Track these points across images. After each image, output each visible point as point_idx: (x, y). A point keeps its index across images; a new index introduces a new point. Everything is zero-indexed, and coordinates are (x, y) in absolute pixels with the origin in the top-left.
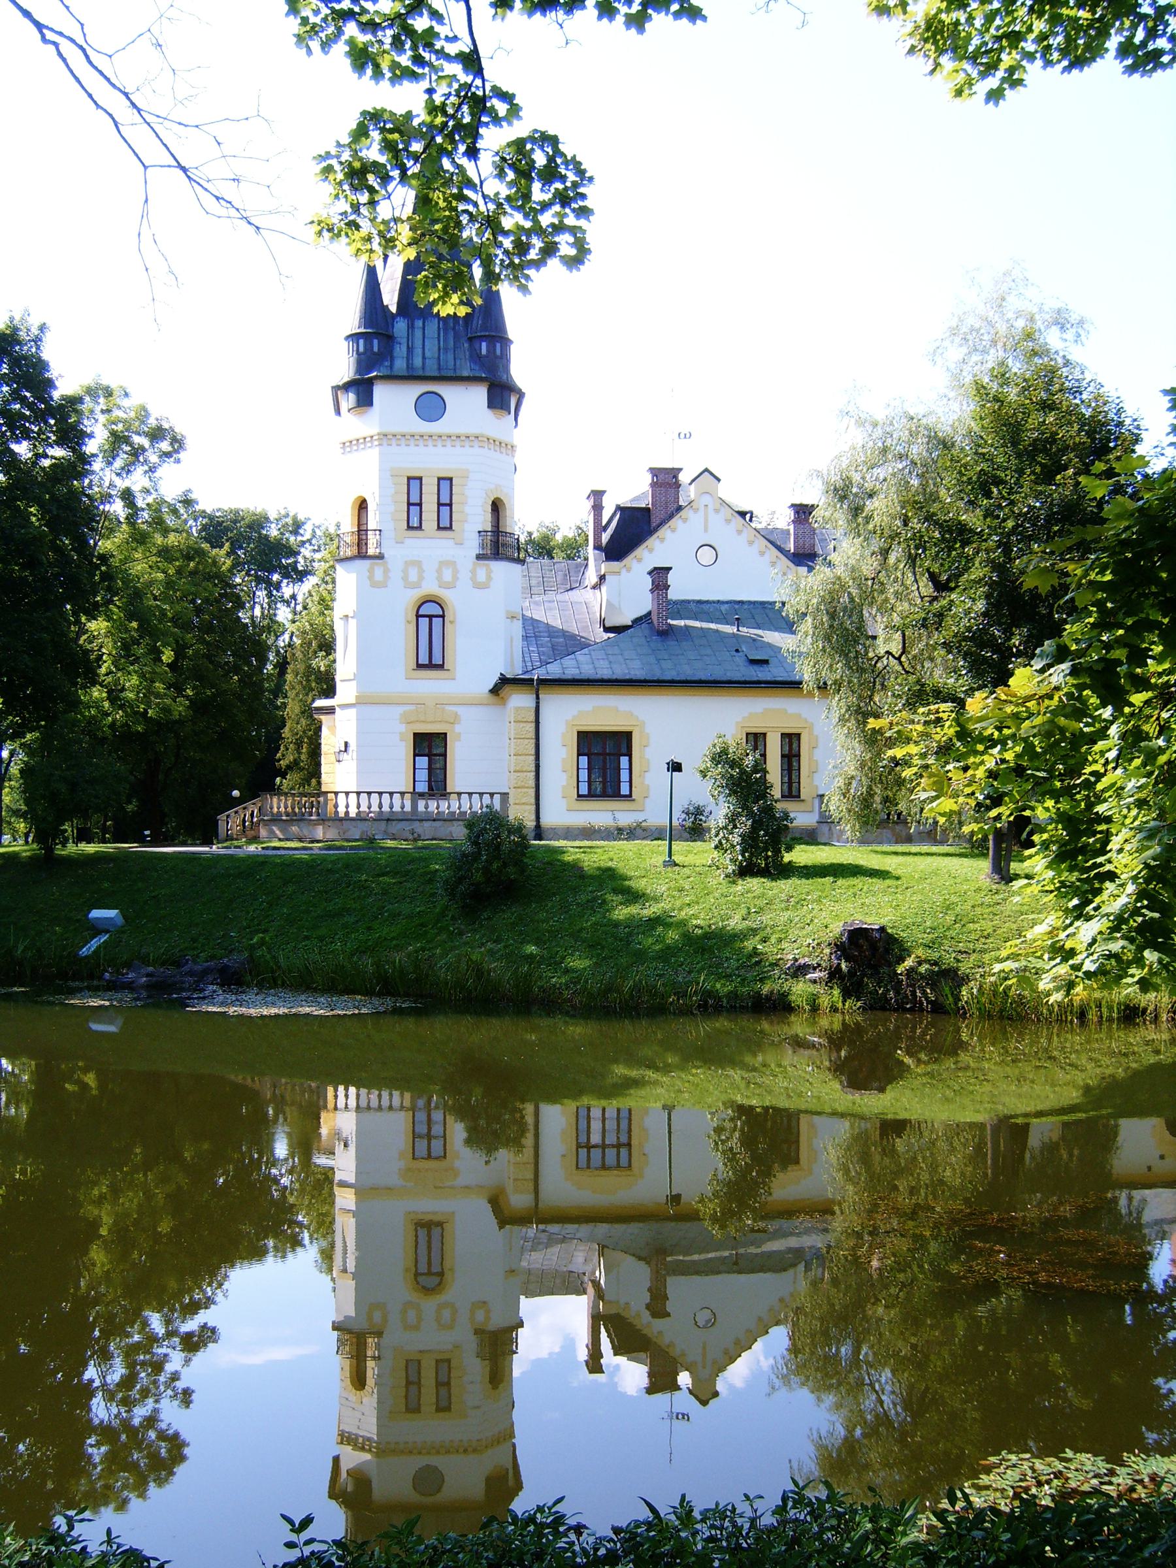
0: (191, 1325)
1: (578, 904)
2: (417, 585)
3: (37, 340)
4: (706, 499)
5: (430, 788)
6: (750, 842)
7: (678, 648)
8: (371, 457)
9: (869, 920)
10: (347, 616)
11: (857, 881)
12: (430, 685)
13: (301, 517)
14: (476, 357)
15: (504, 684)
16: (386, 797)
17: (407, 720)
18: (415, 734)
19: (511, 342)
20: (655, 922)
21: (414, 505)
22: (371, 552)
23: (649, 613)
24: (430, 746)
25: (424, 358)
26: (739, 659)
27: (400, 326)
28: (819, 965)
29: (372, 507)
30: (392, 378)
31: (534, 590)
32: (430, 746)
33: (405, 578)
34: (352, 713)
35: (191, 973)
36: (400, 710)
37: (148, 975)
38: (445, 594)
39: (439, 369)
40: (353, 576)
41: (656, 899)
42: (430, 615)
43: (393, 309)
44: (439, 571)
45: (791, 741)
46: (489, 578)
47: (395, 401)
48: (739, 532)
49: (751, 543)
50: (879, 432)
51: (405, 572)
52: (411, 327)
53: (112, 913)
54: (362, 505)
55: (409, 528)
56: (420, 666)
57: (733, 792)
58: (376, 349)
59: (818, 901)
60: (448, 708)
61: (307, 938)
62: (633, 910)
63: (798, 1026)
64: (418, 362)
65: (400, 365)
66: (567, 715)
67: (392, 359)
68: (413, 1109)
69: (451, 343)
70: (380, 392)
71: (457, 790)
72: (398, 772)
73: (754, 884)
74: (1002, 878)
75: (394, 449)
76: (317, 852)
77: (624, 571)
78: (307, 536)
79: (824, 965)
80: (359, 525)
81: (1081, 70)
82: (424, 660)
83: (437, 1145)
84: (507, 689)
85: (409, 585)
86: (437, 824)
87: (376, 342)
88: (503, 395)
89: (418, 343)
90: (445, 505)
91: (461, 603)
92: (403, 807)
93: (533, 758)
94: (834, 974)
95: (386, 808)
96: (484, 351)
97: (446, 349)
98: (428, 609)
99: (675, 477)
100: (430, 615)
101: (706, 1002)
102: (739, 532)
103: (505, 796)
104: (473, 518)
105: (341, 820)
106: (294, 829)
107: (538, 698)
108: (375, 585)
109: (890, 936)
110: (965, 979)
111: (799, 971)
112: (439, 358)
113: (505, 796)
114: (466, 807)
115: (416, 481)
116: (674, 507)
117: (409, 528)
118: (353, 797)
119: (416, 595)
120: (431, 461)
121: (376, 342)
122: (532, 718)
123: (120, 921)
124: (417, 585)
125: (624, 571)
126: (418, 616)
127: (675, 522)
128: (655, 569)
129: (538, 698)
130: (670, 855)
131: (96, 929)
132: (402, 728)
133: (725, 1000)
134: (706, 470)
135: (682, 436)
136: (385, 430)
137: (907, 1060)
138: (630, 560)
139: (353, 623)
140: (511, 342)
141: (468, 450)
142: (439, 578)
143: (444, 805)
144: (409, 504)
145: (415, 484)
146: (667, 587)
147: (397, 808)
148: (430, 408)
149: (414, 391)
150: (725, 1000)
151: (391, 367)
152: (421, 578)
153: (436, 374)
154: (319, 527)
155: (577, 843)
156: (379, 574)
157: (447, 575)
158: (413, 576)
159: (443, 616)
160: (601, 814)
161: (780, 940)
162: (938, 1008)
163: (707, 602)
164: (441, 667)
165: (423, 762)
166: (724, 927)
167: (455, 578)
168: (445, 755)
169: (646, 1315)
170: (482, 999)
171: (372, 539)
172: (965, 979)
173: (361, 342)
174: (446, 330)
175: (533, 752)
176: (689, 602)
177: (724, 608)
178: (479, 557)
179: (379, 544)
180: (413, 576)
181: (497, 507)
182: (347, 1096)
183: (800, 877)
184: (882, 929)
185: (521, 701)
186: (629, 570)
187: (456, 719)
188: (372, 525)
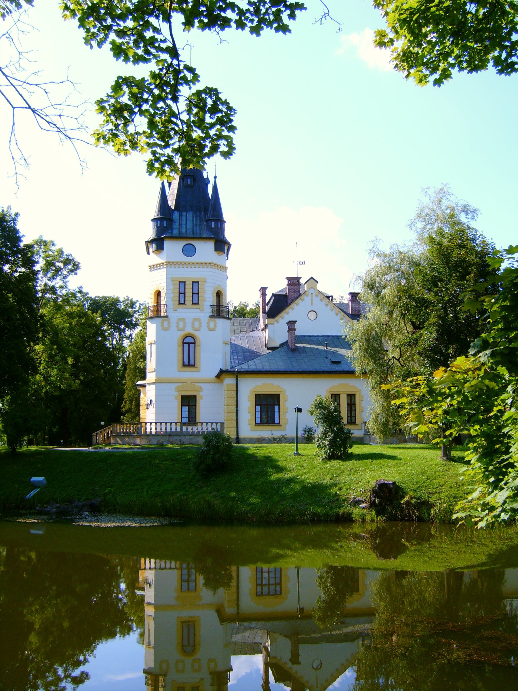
0: (76, 673)
1: (255, 474)
3: (14, 220)
4: (312, 291)
5: (189, 420)
6: (333, 444)
7: (301, 357)
8: (162, 273)
9: (388, 479)
10: (151, 343)
11: (382, 461)
12: (188, 374)
13: (134, 300)
14: (209, 229)
15: (222, 374)
16: (168, 425)
17: (178, 390)
18: (182, 396)
19: (225, 222)
20: (291, 480)
21: (182, 293)
22: (162, 314)
23: (287, 341)
24: (189, 402)
25: (186, 229)
26: (327, 361)
27: (176, 215)
28: (365, 500)
29: (163, 294)
31: (236, 332)
32: (189, 402)
33: (178, 326)
34: (153, 387)
35: (77, 507)
36: (176, 385)
37: (57, 508)
38: (196, 333)
39: (193, 233)
40: (155, 325)
41: (290, 471)
42: (189, 343)
43: (173, 207)
44: (193, 323)
45: (351, 398)
46: (215, 326)
47: (173, 248)
48: (327, 305)
49: (332, 310)
50: (387, 259)
51: (178, 323)
52: (181, 216)
53: (41, 479)
54: (158, 294)
55: (180, 304)
56: (184, 365)
57: (325, 421)
58: (165, 225)
59: (365, 471)
60: (197, 384)
61: (131, 490)
62: (280, 475)
63: (356, 529)
64: (184, 231)
65: (176, 232)
66: (250, 388)
68: (181, 568)
69: (198, 223)
70: (167, 244)
71: (201, 421)
72: (175, 413)
73: (335, 463)
74: (448, 459)
76: (136, 450)
77: (276, 323)
78: (137, 309)
79: (367, 500)
80: (157, 303)
81: (477, 72)
82: (187, 363)
83: (192, 585)
84: (224, 375)
85: (179, 329)
86: (192, 437)
87: (165, 222)
88: (222, 245)
89: (184, 222)
90: (196, 294)
91: (203, 337)
92: (176, 429)
93: (235, 406)
94: (373, 504)
95: (168, 430)
96: (213, 226)
97: (196, 225)
98: (188, 340)
99: (298, 281)
100: (189, 343)
101: (314, 518)
102: (327, 305)
103: (222, 424)
104: (208, 299)
105: (148, 435)
106: (127, 439)
107: (237, 379)
108: (164, 329)
109: (398, 486)
110: (432, 506)
111: (356, 503)
112: (193, 229)
113: (222, 424)
114: (205, 429)
115: (182, 283)
116: (297, 294)
117: (180, 304)
118: (154, 425)
119: (182, 334)
120: (190, 274)
121: (165, 222)
122: (235, 388)
123: (45, 482)
125: (276, 323)
126: (183, 343)
127: (298, 301)
128: (290, 321)
129: (237, 379)
130: (297, 450)
131: (34, 486)
132: (176, 393)
133: (323, 518)
134: (312, 278)
135: (301, 263)
136: (169, 261)
137: (407, 544)
138: (278, 318)
139: (154, 346)
140: (225, 222)
141: (205, 269)
142: (193, 326)
143: (195, 428)
144: (180, 293)
145: (182, 285)
146: (295, 330)
147: (173, 430)
148: (189, 251)
149: (182, 243)
150: (323, 518)
151: (172, 233)
152: (185, 326)
154: (142, 305)
155: (255, 445)
156: (166, 324)
157: (197, 325)
158: (181, 325)
159: (195, 343)
160: (266, 432)
161: (347, 489)
162: (420, 519)
163: (313, 336)
164: (194, 366)
165: (186, 409)
166: (322, 483)
167: (200, 326)
168: (196, 406)
169: (290, 664)
170: (210, 518)
171: (163, 309)
172: (432, 506)
173: (159, 222)
174: (196, 217)
175: (235, 404)
176: (305, 336)
177: (320, 339)
178: (211, 317)
179: (166, 311)
180: (181, 325)
181: (219, 295)
182: (150, 563)
183: (356, 460)
184: (394, 483)
185: (230, 381)
186: (278, 322)
187: (200, 389)
188: (163, 302)
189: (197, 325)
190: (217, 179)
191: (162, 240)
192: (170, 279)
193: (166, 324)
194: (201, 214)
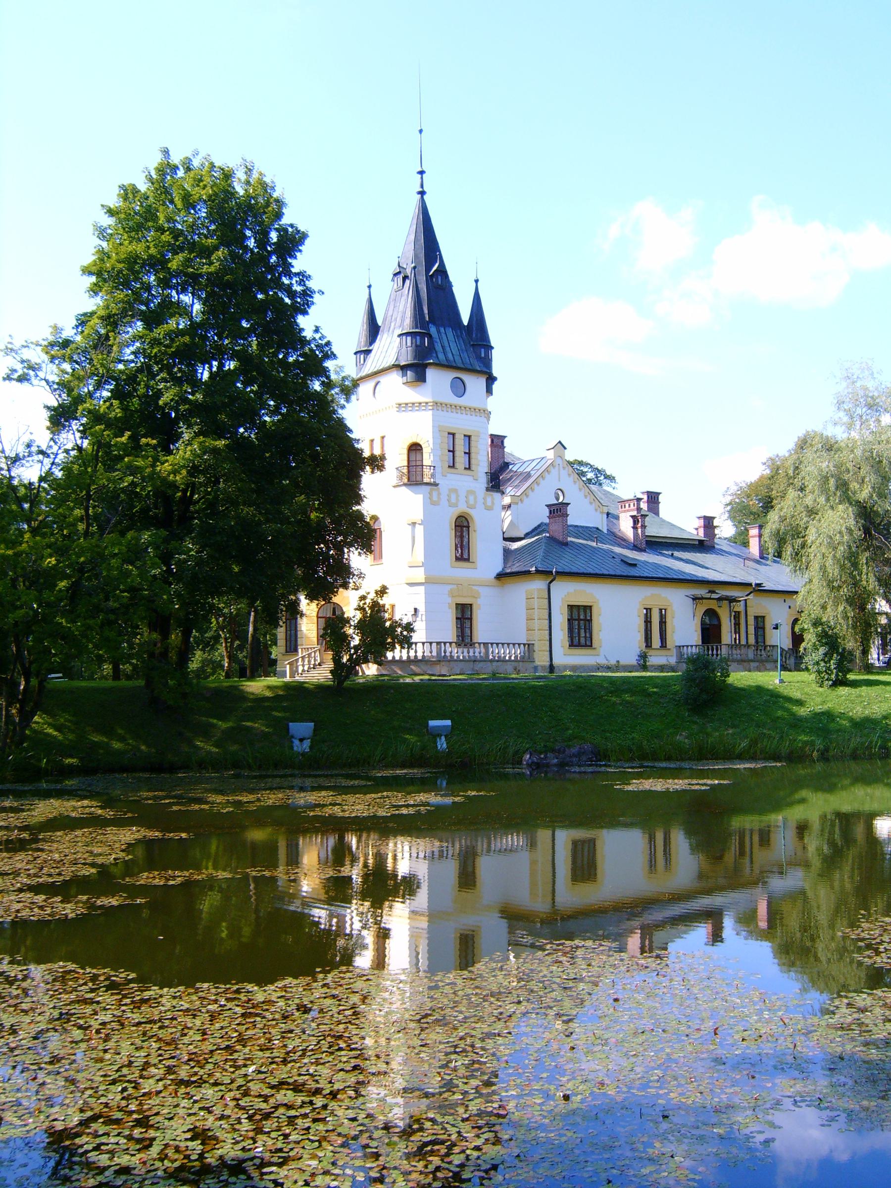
2: (456, 505)
10: (414, 524)
12: (463, 572)
14: (479, 358)
17: (452, 594)
19: (492, 348)
22: (426, 480)
27: (433, 330)
29: (426, 450)
30: (439, 365)
32: (464, 615)
36: (449, 587)
38: (472, 512)
40: (421, 496)
42: (462, 526)
46: (493, 503)
54: (415, 448)
60: (474, 587)
66: (567, 592)
67: (436, 353)
70: (430, 373)
75: (440, 412)
89: (446, 344)
96: (483, 355)
99: (502, 442)
100: (462, 526)
107: (550, 582)
108: (433, 503)
113: (529, 646)
116: (501, 461)
119: (454, 513)
120: (462, 423)
122: (547, 596)
124: (456, 505)
131: (435, 735)
132: (449, 600)
134: (560, 442)
136: (436, 400)
140: (492, 348)
148: (459, 388)
153: (462, 366)
159: (468, 527)
164: (468, 560)
167: (476, 502)
168: (471, 619)
173: (418, 338)
179: (433, 476)
180: (453, 497)
189: (472, 502)
190: (479, 283)
191: (426, 366)
192: (438, 429)
193: (435, 498)
194: (461, 333)
